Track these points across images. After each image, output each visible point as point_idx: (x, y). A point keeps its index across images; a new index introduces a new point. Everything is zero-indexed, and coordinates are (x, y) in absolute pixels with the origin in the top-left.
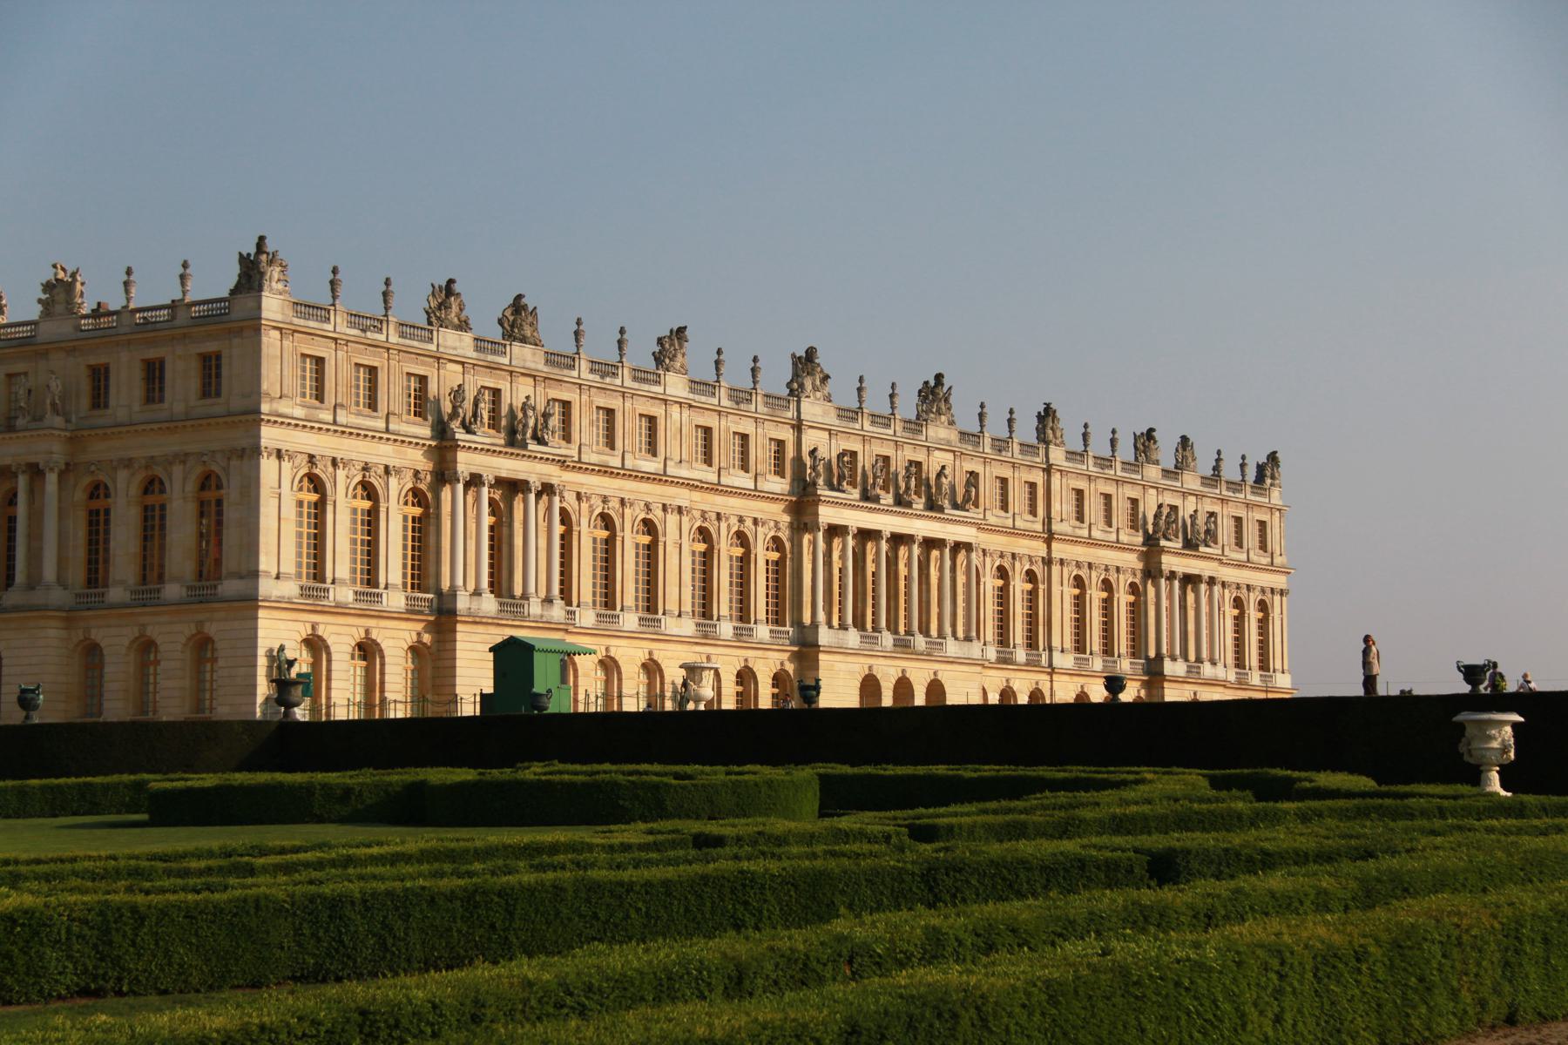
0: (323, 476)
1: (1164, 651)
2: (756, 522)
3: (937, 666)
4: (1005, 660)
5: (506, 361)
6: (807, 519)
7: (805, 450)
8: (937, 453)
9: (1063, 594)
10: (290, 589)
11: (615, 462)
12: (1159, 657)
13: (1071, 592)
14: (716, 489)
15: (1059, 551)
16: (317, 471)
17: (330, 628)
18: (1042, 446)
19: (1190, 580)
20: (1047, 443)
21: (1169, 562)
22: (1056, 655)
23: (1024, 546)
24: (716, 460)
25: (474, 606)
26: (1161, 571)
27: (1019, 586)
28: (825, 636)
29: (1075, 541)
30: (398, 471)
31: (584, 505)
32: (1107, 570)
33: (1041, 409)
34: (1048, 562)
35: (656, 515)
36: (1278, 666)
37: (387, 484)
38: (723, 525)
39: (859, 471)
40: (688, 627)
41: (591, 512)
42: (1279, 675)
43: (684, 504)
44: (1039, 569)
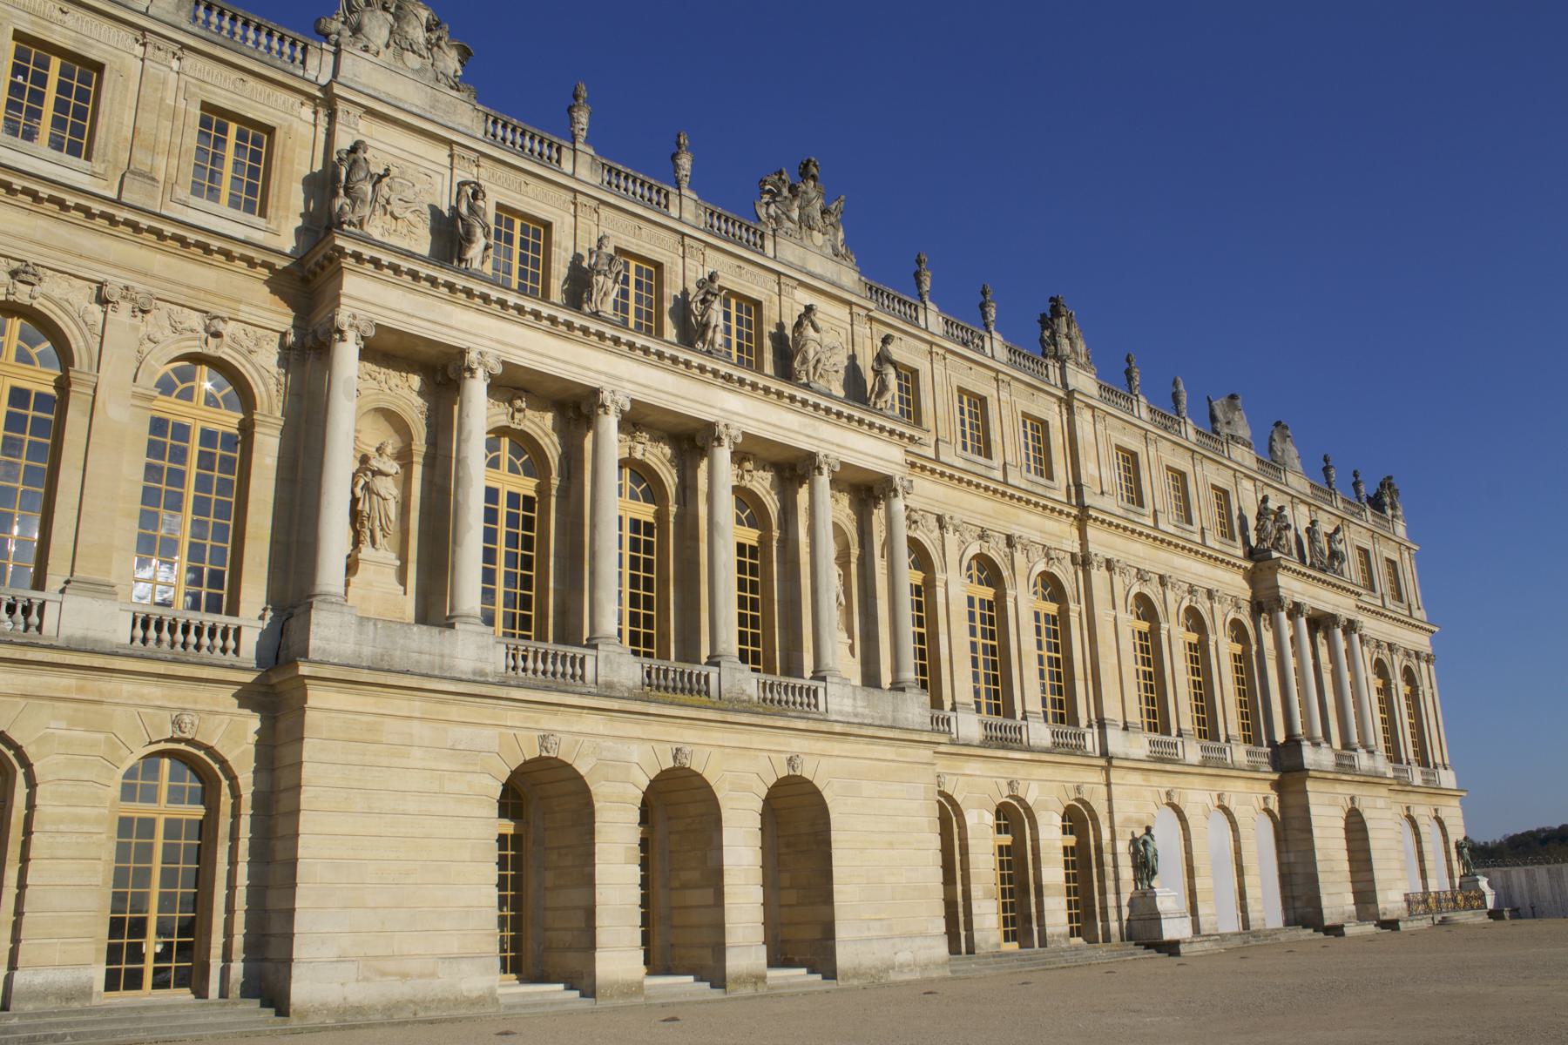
1: (1299, 730)
3: (797, 744)
4: (1003, 739)
9: (1117, 631)
12: (1293, 742)
13: (1131, 624)
19: (1321, 623)
20: (1062, 360)
21: (1291, 586)
23: (1029, 524)
26: (1279, 601)
27: (1025, 604)
28: (329, 633)
32: (1192, 591)
36: (1438, 760)
42: (1441, 771)
44: (1067, 575)
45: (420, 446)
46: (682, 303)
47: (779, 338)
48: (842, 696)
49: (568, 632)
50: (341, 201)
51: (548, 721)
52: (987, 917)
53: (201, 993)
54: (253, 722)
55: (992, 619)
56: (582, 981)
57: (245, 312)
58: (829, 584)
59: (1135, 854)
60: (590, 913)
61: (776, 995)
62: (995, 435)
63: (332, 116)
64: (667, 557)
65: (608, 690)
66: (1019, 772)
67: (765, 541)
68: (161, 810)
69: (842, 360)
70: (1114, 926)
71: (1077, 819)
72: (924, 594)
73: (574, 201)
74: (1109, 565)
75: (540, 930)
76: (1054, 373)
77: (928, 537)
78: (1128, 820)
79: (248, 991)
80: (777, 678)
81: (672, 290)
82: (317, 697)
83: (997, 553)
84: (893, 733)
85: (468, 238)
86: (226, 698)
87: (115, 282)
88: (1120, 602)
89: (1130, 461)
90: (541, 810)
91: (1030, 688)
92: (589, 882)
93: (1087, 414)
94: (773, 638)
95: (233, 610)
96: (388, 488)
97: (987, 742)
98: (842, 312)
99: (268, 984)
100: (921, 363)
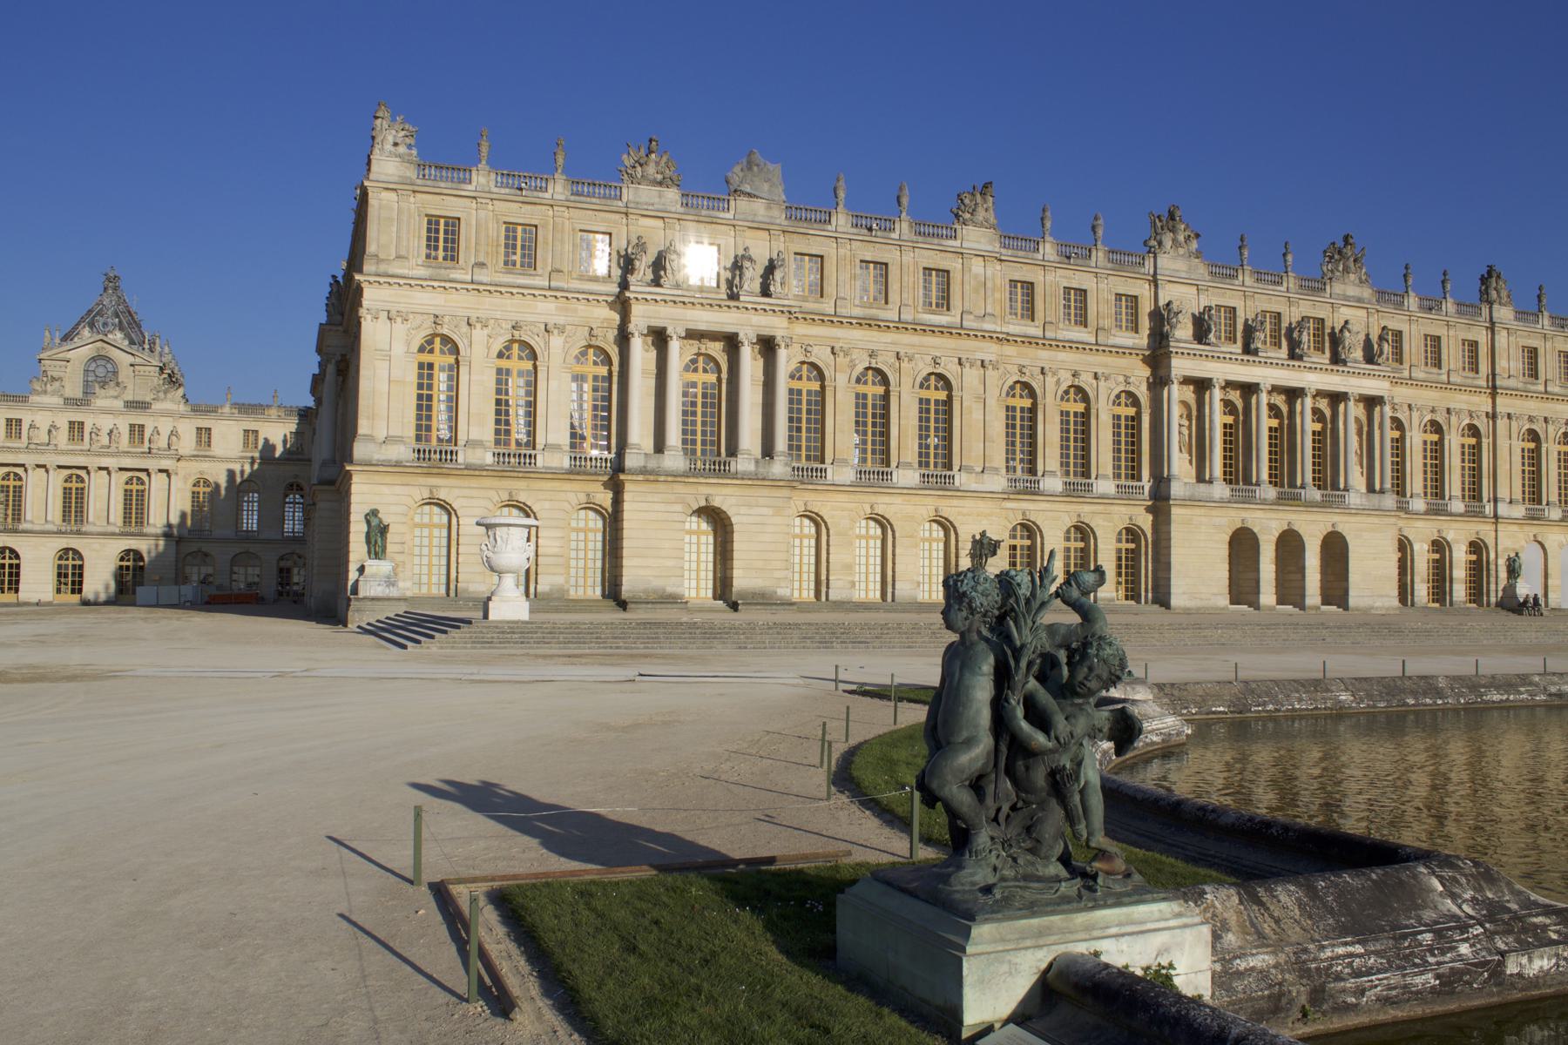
0: (455, 337)
2: (1096, 377)
3: (1336, 518)
4: (1437, 510)
5: (730, 215)
6: (1162, 372)
7: (1162, 303)
8: (1343, 310)
10: (403, 452)
11: (891, 314)
14: (1029, 341)
15: (1503, 404)
16: (445, 331)
17: (456, 492)
18: (1485, 310)
20: (1491, 303)
22: (1500, 505)
23: (1460, 401)
24: (1039, 313)
25: (652, 464)
27: (1455, 442)
28: (1176, 489)
29: (1525, 394)
30: (561, 330)
31: (840, 359)
33: (1484, 271)
34: (1493, 416)
35: (950, 369)
37: (547, 343)
38: (1050, 380)
39: (1240, 327)
40: (999, 482)
41: (853, 366)
43: (987, 358)
44: (1482, 424)
45: (1194, 413)
46: (1290, 330)
47: (1332, 335)
48: (1356, 497)
49: (1247, 481)
50: (1167, 328)
51: (1244, 514)
52: (1422, 591)
53: (1139, 602)
54: (1150, 517)
55: (1436, 451)
56: (1255, 604)
57: (1137, 372)
58: (1352, 443)
59: (1509, 567)
60: (1258, 582)
61: (1324, 613)
62: (1444, 356)
63: (1156, 286)
64: (1284, 441)
65: (1264, 502)
66: (1445, 526)
67: (1324, 429)
68: (1124, 546)
69: (1362, 337)
70: (1493, 600)
71: (1476, 547)
72: (1399, 445)
73: (1248, 298)
74: (1509, 416)
75: (1242, 588)
76: (1485, 310)
77: (1403, 416)
78: (1506, 549)
79: (1154, 602)
80: (1329, 492)
81: (1285, 325)
82: (1175, 511)
83: (1440, 418)
84: (1380, 511)
85: (1209, 330)
86: (1142, 510)
87: (1100, 371)
88: (1514, 436)
89: (1532, 354)
90: (1243, 545)
91: (1455, 483)
92: (1257, 570)
93: (1504, 333)
94: (1328, 477)
95: (1140, 479)
96: (1186, 432)
97: (1426, 513)
98: (1363, 313)
99: (1162, 598)
100: (1404, 327)
